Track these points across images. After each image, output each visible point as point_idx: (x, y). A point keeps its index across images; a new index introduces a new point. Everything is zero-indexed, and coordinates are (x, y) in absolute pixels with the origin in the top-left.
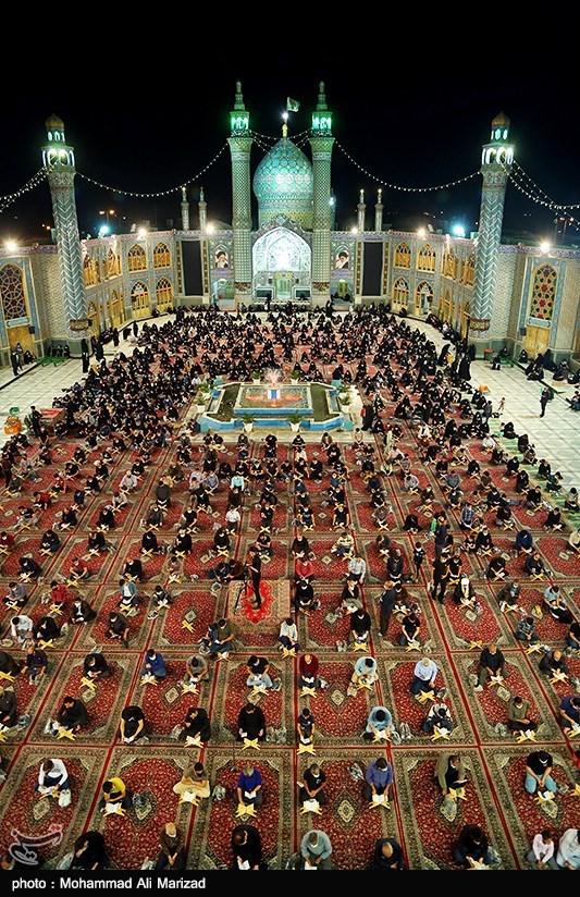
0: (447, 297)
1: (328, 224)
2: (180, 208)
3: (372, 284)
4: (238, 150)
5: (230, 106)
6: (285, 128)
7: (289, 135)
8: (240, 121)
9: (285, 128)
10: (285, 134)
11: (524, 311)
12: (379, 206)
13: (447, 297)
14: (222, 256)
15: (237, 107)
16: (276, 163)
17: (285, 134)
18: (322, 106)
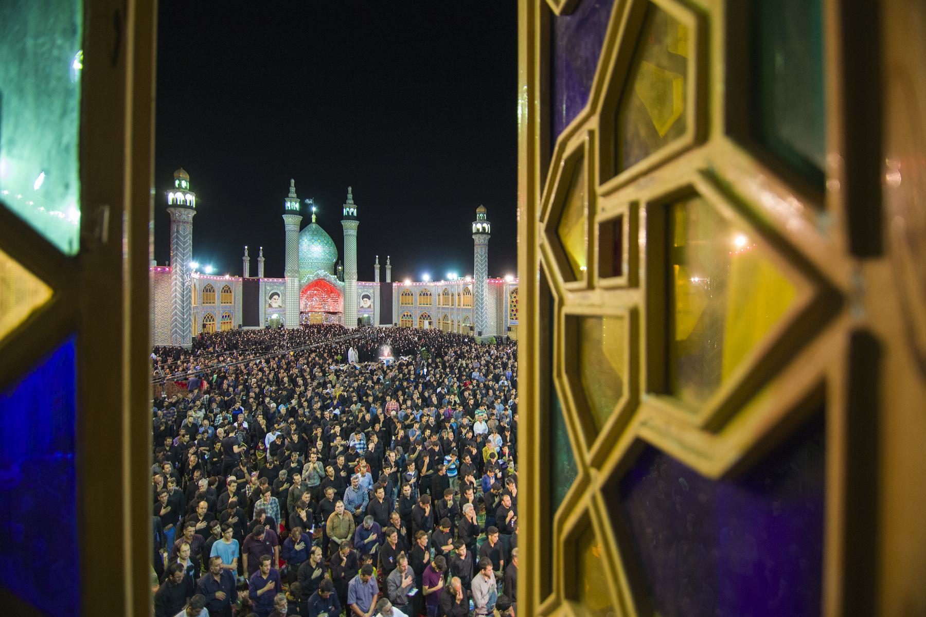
0: (445, 317)
1: (356, 277)
2: (242, 262)
3: (386, 316)
4: (291, 222)
5: (286, 194)
6: (314, 217)
7: (317, 221)
8: (293, 204)
9: (314, 217)
10: (314, 220)
11: (506, 316)
12: (388, 267)
13: (445, 317)
14: (276, 297)
15: (290, 195)
16: (309, 237)
17: (314, 220)
18: (352, 202)
